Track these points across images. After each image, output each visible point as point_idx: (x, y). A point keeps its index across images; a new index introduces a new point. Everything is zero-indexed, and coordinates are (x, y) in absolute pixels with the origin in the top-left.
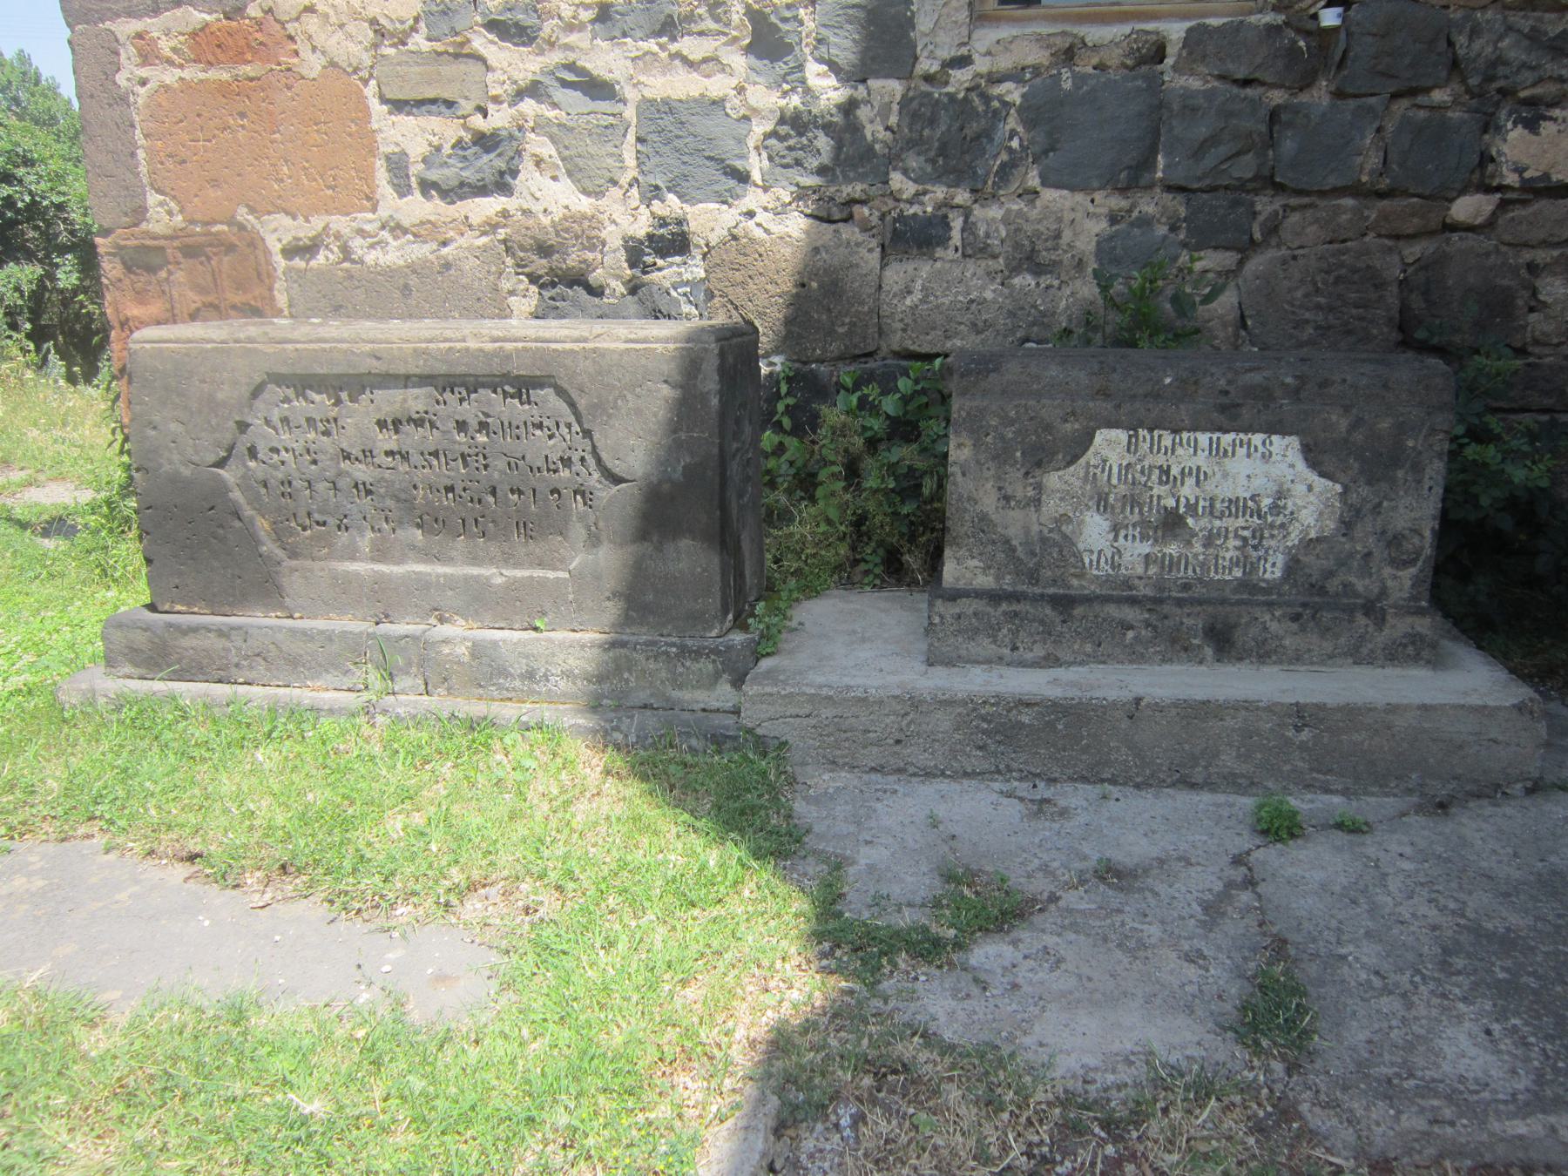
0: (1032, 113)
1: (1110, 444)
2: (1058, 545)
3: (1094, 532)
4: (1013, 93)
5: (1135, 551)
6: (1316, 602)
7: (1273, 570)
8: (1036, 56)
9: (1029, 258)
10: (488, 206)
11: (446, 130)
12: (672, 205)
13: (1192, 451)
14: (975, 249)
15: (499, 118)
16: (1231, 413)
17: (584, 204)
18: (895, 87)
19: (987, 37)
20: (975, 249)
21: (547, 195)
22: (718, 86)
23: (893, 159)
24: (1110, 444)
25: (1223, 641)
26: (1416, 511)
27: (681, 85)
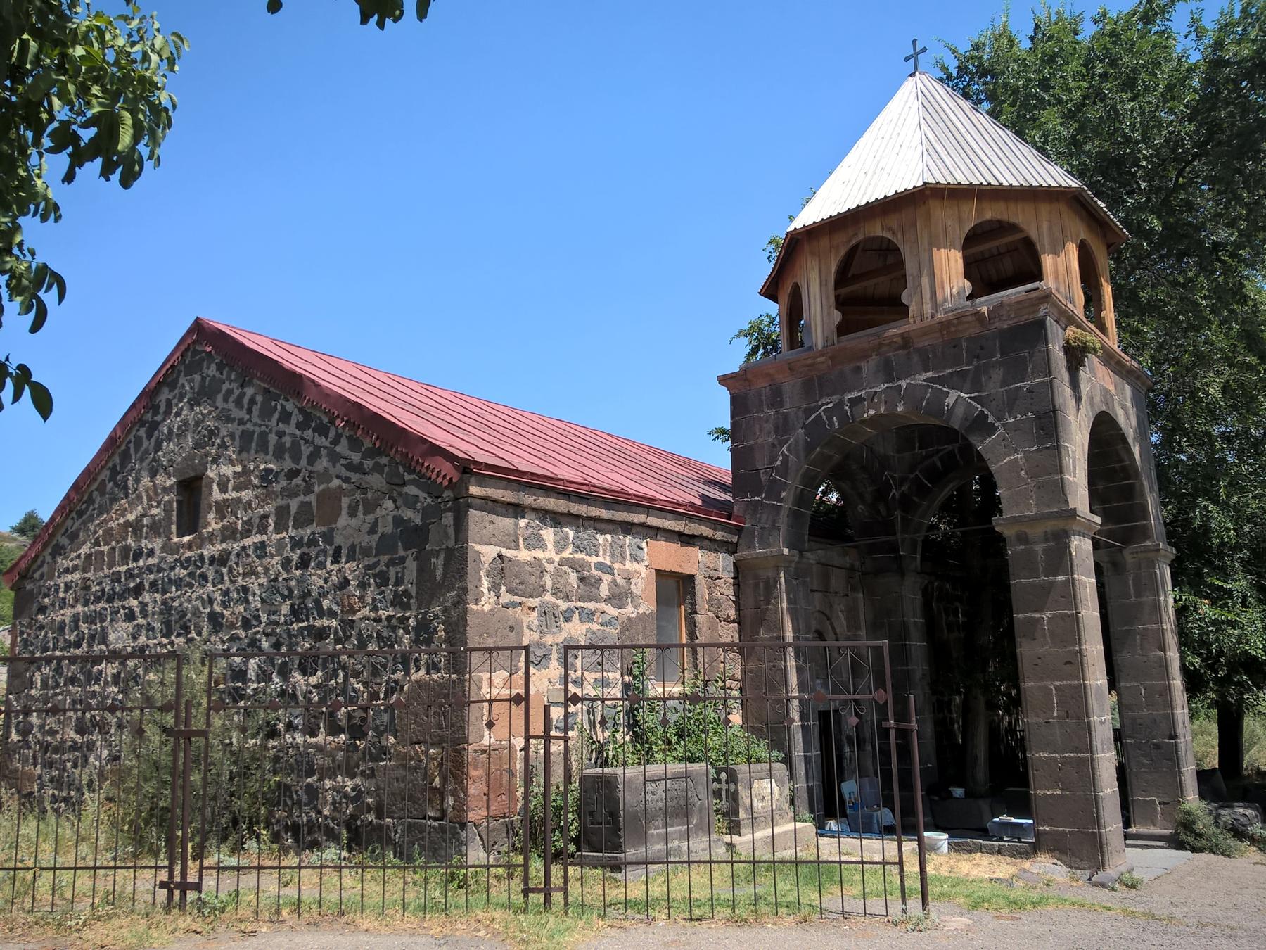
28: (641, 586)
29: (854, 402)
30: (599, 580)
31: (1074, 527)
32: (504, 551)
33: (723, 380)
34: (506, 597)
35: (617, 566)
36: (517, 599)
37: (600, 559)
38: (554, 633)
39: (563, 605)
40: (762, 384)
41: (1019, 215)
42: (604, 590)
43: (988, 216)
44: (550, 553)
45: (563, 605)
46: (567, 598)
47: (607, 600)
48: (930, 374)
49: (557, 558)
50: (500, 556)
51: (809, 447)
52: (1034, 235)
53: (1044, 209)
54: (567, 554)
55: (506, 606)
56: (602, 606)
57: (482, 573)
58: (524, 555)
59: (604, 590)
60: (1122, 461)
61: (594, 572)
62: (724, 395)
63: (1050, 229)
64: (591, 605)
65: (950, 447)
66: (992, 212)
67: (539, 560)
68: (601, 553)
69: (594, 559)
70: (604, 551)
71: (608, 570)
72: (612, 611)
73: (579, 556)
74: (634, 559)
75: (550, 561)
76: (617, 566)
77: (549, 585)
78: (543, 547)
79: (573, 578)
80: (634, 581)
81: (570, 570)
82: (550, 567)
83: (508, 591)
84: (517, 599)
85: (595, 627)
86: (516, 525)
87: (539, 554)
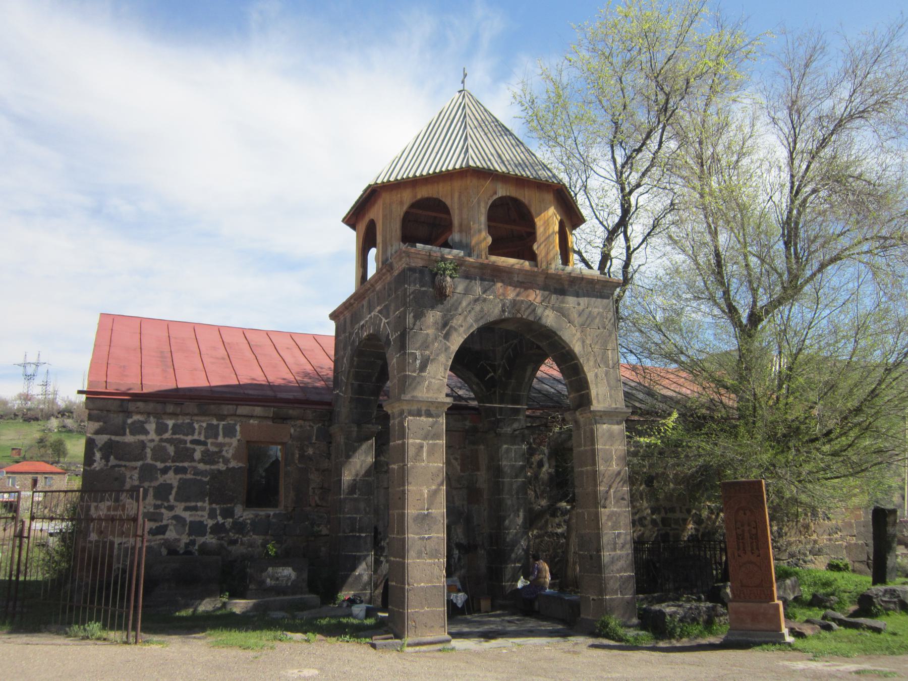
0: (251, 524)
1: (270, 569)
2: (264, 582)
3: (268, 580)
4: (249, 521)
5: (273, 582)
6: (294, 588)
7: (289, 584)
8: (251, 516)
9: (251, 545)
10: (161, 537)
11: (153, 525)
12: (193, 537)
13: (280, 570)
14: (242, 544)
15: (165, 522)
16: (285, 565)
17: (178, 537)
18: (231, 520)
19: (245, 514)
20: (242, 544)
21: (171, 534)
22: (202, 519)
23: (230, 530)
24: (270, 569)
25: (285, 594)
26: (305, 576)
27: (198, 519)
28: (231, 451)
29: (363, 326)
30: (194, 450)
31: (406, 407)
32: (113, 438)
33: (334, 316)
34: (113, 461)
35: (209, 441)
36: (123, 463)
37: (196, 437)
38: (151, 481)
39: (160, 465)
40: (342, 318)
41: (438, 191)
42: (197, 455)
43: (419, 197)
44: (153, 435)
45: (160, 465)
46: (163, 461)
47: (200, 461)
48: (379, 308)
49: (157, 438)
50: (110, 439)
51: (352, 360)
52: (448, 202)
53: (457, 184)
54: (166, 436)
55: (113, 467)
56: (194, 464)
57: (95, 450)
58: (129, 438)
59: (197, 455)
60: (564, 348)
61: (189, 445)
62: (332, 325)
63: (460, 197)
64: (186, 464)
65: (515, 341)
66: (423, 192)
67: (143, 442)
68: (197, 433)
69: (189, 438)
70: (200, 434)
71: (204, 443)
72: (201, 466)
73: (177, 436)
74: (225, 436)
75: (153, 441)
76: (209, 441)
77: (148, 451)
78: (146, 433)
79: (171, 450)
80: (225, 449)
81: (168, 445)
82: (149, 444)
83: (116, 458)
84: (123, 463)
85: (189, 476)
86: (125, 422)
87: (142, 437)
